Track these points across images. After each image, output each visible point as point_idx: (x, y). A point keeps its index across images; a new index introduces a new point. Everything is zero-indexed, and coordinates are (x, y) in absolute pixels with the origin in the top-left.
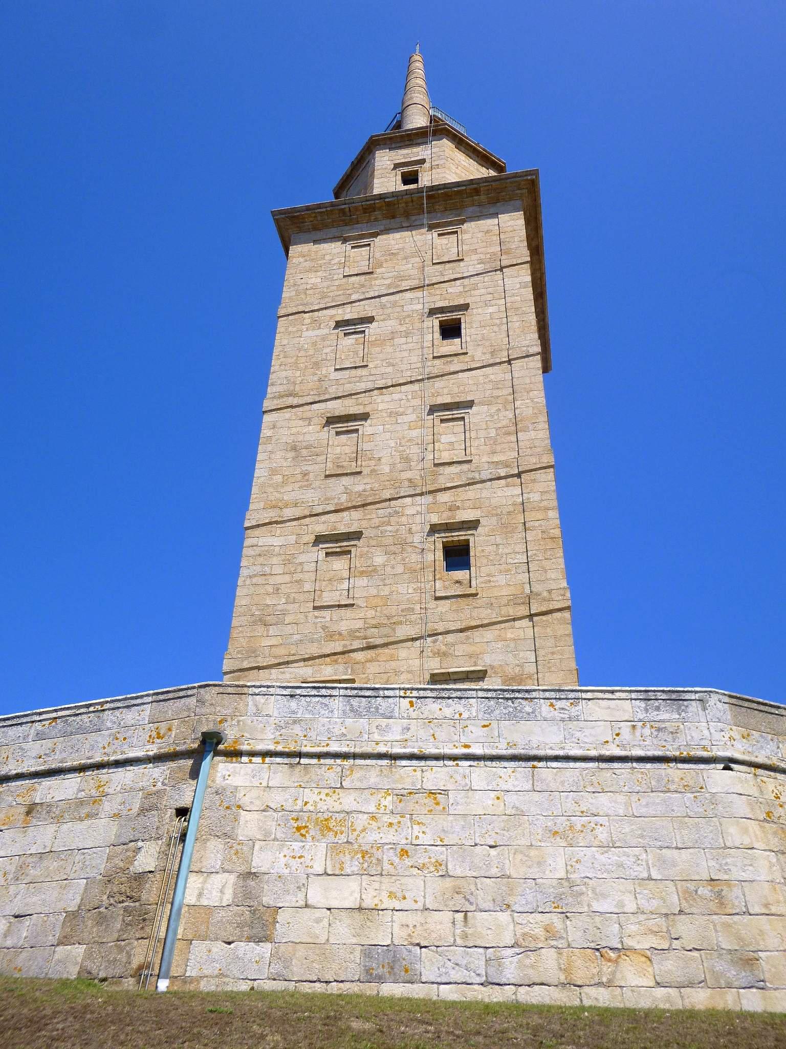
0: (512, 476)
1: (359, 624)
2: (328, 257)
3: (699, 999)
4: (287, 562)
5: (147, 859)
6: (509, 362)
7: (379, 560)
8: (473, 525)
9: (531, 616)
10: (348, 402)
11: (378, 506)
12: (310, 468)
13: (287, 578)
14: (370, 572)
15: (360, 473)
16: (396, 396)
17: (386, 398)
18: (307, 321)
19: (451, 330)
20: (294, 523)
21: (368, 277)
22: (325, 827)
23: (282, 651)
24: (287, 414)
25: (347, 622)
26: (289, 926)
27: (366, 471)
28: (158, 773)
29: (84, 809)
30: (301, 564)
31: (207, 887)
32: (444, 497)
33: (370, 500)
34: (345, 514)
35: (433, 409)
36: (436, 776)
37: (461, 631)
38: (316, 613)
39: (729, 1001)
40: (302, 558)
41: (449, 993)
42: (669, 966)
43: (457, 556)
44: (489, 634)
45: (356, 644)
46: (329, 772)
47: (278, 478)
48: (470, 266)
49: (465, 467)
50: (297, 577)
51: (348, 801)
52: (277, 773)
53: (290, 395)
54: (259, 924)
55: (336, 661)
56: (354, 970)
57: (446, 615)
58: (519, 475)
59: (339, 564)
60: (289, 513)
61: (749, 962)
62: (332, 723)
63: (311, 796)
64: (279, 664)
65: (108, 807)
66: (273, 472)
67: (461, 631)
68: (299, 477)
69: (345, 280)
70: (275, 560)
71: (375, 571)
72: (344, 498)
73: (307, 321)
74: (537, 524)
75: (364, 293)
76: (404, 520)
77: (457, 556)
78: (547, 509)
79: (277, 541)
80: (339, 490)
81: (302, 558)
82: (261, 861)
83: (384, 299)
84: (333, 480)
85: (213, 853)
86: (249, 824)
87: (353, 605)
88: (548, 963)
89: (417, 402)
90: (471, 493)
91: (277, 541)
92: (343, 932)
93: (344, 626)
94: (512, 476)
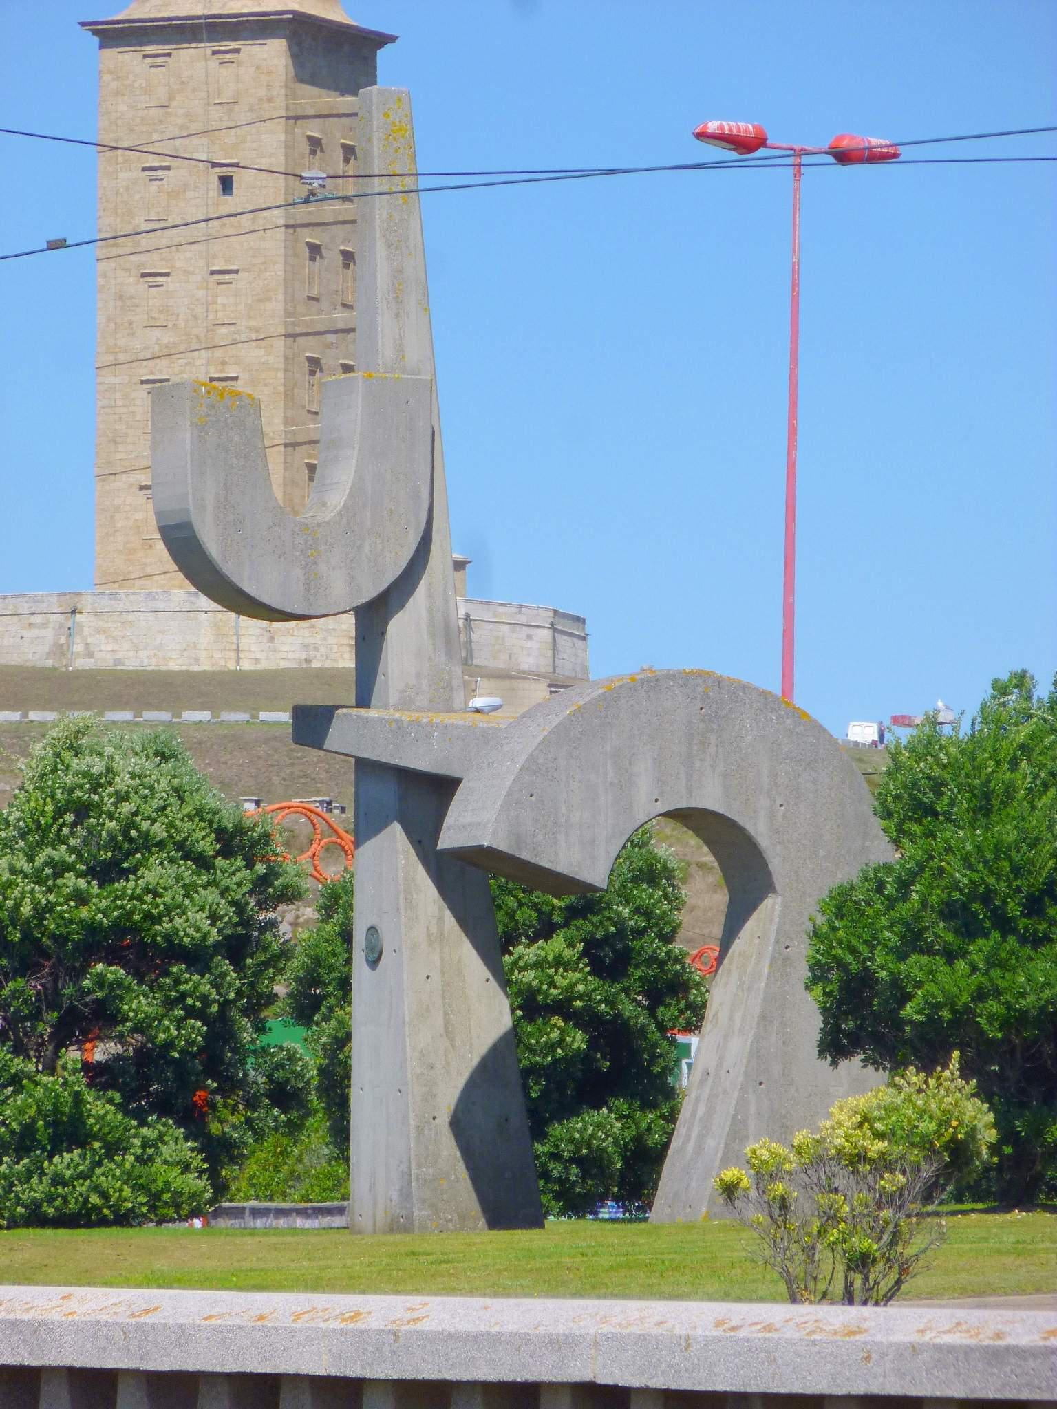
2: (131, 76)
3: (184, 668)
5: (63, 640)
8: (236, 379)
13: (125, 410)
16: (188, 255)
18: (120, 160)
21: (161, 111)
22: (104, 631)
26: (96, 655)
27: (170, 325)
28: (62, 617)
29: (44, 625)
31: (78, 647)
32: (218, 353)
33: (173, 351)
34: (157, 361)
36: (131, 617)
39: (191, 668)
40: (134, 395)
41: (131, 668)
42: (180, 662)
46: (105, 616)
49: (232, 328)
50: (131, 409)
51: (110, 625)
52: (92, 618)
54: (90, 655)
56: (111, 663)
60: (122, 357)
61: (197, 660)
62: (105, 603)
63: (101, 623)
65: (51, 625)
66: (109, 319)
70: (118, 395)
72: (157, 348)
73: (120, 160)
75: (162, 133)
76: (194, 369)
78: (278, 370)
79: (117, 380)
81: (134, 395)
82: (89, 640)
85: (78, 639)
86: (86, 631)
88: (154, 661)
89: (202, 263)
90: (233, 351)
91: (117, 380)
92: (109, 656)
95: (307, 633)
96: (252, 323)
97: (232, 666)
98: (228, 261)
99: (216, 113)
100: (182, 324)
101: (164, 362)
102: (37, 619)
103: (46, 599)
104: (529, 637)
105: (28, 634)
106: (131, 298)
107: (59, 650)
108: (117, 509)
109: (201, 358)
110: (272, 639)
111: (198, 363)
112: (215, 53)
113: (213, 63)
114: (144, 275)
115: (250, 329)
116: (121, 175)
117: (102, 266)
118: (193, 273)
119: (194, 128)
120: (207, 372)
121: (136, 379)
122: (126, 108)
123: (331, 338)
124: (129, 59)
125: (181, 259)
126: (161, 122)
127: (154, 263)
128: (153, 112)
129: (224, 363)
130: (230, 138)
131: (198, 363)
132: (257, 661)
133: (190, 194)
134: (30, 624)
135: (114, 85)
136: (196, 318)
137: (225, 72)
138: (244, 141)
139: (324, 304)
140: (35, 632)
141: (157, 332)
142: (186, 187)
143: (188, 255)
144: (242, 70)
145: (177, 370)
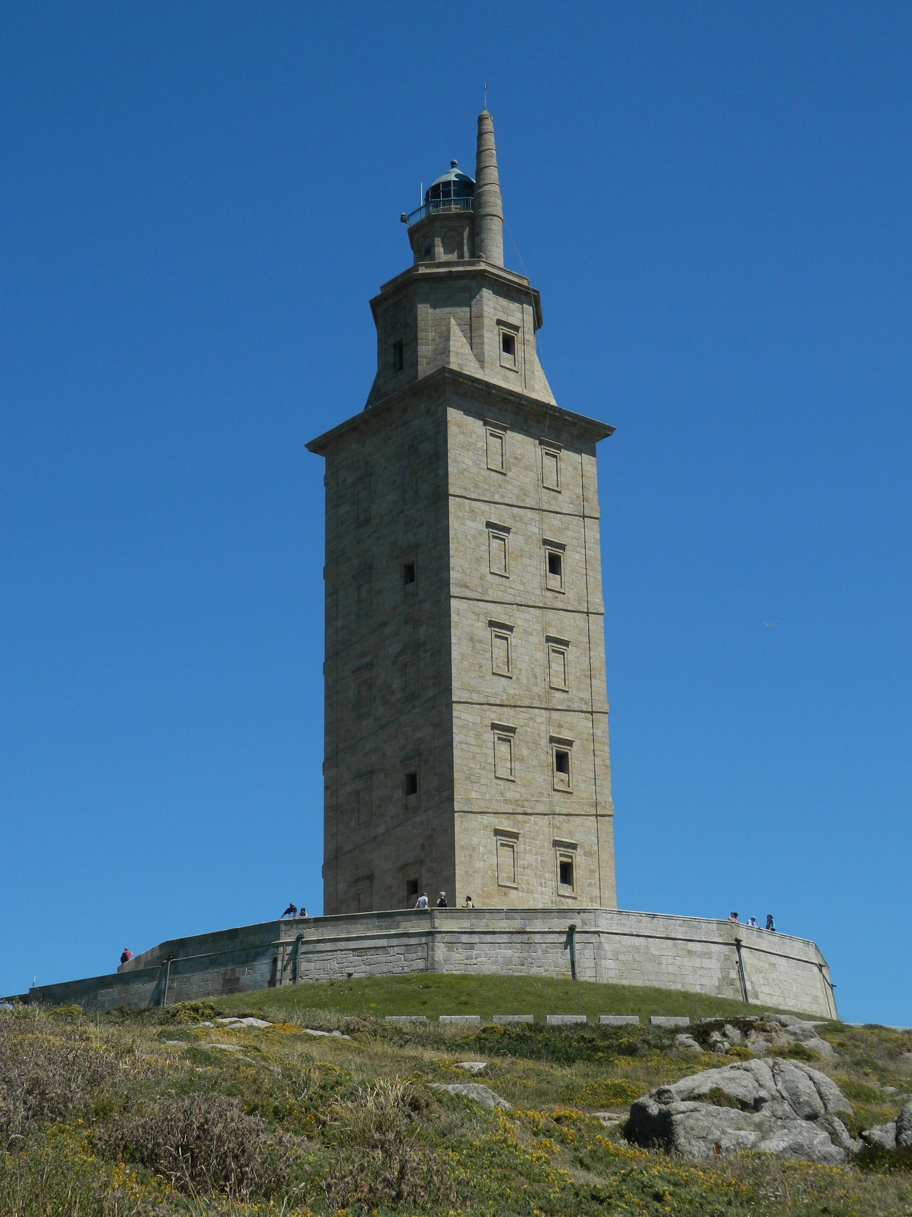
0: (588, 712)
1: (517, 796)
4: (478, 736)
6: (588, 613)
7: (525, 752)
9: (597, 816)
10: (500, 608)
11: (522, 709)
12: (483, 662)
14: (522, 760)
15: (511, 678)
16: (528, 616)
17: (521, 614)
20: (478, 706)
23: (482, 804)
25: (513, 792)
27: (514, 678)
29: (709, 955)
30: (485, 741)
33: (519, 703)
34: (505, 709)
35: (549, 639)
37: (566, 815)
38: (497, 781)
44: (578, 820)
45: (519, 810)
48: (564, 502)
49: (565, 695)
50: (484, 750)
53: (467, 587)
55: (509, 818)
57: (561, 803)
58: (592, 713)
59: (503, 748)
60: (476, 698)
64: (481, 813)
67: (566, 815)
68: (477, 667)
69: (488, 472)
71: (523, 759)
74: (600, 753)
76: (536, 725)
77: (562, 762)
84: (496, 677)
87: (514, 781)
89: (538, 627)
91: (470, 718)
93: (509, 795)
94: (588, 712)
100: (525, 681)
101: (511, 711)
103: (703, 925)
105: (687, 962)
106: (480, 641)
108: (474, 849)
109: (541, 716)
111: (539, 720)
118: (531, 634)
120: (548, 731)
121: (488, 722)
122: (470, 463)
126: (500, 486)
128: (493, 474)
131: (539, 720)
134: (689, 951)
136: (536, 677)
138: (567, 529)
140: (698, 962)
143: (528, 616)
145: (522, 721)
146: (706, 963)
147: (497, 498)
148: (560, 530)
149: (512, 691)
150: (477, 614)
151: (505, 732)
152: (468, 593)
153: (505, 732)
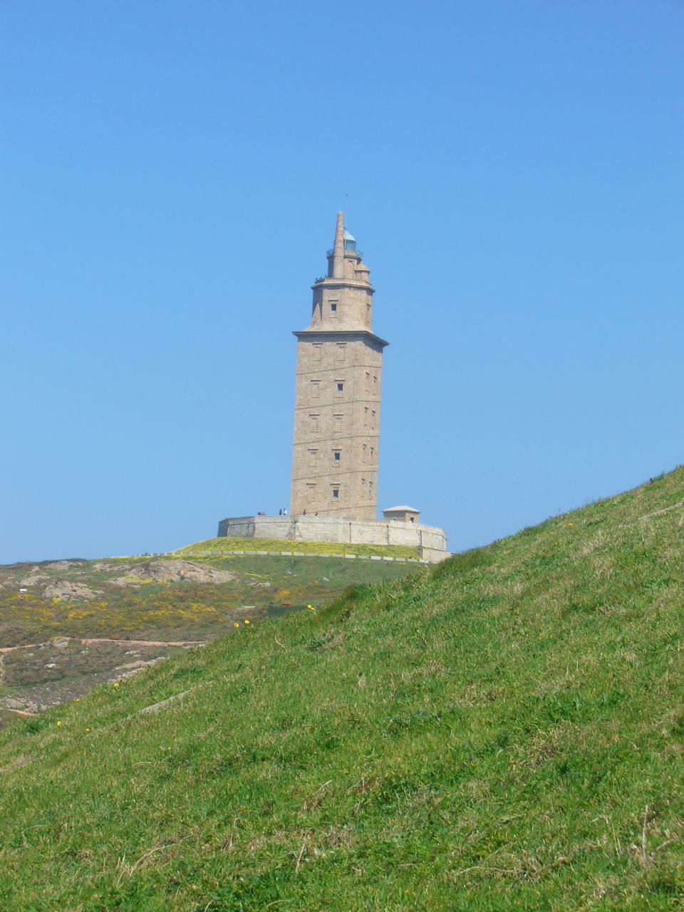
7: (322, 456)
10: (315, 409)
14: (320, 459)
19: (340, 387)
24: (301, 411)
31: (297, 534)
32: (336, 441)
43: (337, 456)
44: (341, 476)
47: (299, 432)
48: (346, 364)
54: (301, 536)
59: (313, 456)
60: (303, 442)
66: (298, 429)
77: (337, 456)
80: (314, 436)
83: (324, 373)
93: (315, 471)
95: (372, 532)
96: (348, 432)
97: (348, 542)
98: (341, 412)
99: (337, 364)
100: (323, 431)
101: (317, 444)
102: (283, 524)
104: (437, 538)
107: (290, 535)
109: (330, 443)
110: (361, 534)
112: (338, 344)
113: (338, 347)
114: (311, 415)
115: (347, 434)
116: (304, 382)
117: (297, 411)
119: (330, 368)
123: (369, 438)
124: (308, 345)
125: (324, 411)
127: (315, 411)
129: (337, 445)
130: (342, 372)
132: (357, 540)
133: (328, 390)
135: (303, 353)
136: (328, 429)
137: (340, 350)
139: (368, 428)
140: (282, 528)
141: (315, 434)
142: (326, 387)
144: (346, 350)
146: (285, 528)
147: (316, 370)
148: (344, 375)
149: (317, 437)
150: (305, 414)
151: (314, 451)
152: (302, 407)
153: (314, 451)
